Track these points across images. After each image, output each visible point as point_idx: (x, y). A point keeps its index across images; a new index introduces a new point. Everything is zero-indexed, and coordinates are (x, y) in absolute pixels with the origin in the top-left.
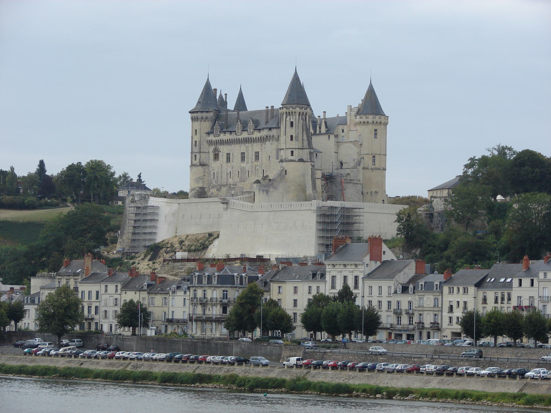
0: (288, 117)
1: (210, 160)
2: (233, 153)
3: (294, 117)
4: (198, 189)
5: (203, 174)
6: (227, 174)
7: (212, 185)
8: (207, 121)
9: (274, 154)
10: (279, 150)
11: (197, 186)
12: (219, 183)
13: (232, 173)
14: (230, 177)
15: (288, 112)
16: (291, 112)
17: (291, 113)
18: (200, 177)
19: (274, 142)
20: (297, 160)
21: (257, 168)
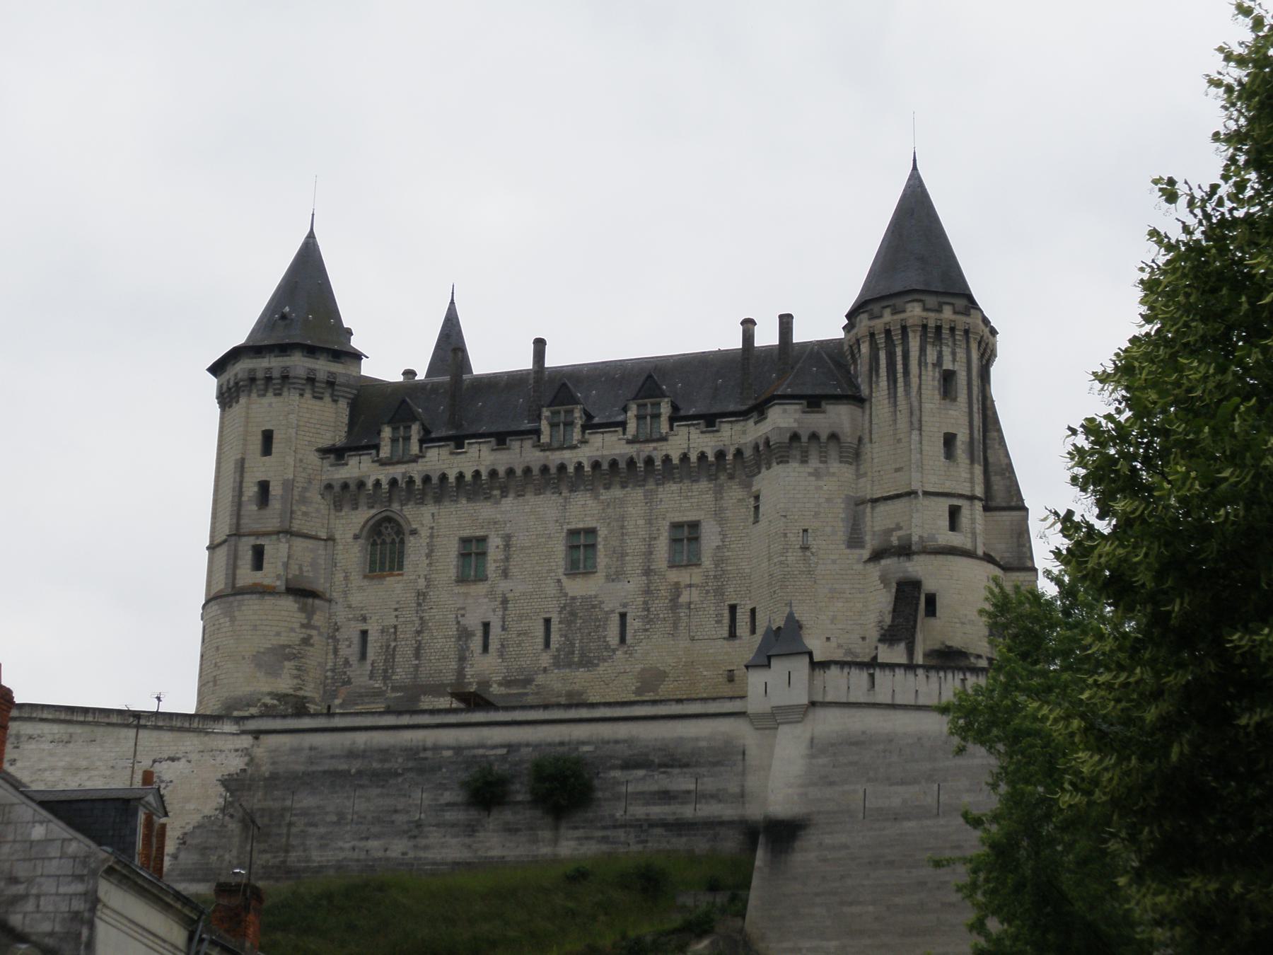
0: (931, 355)
1: (339, 576)
2: (507, 538)
3: (961, 354)
4: (268, 700)
5: (303, 633)
6: (464, 634)
7: (344, 691)
8: (327, 398)
9: (835, 522)
10: (859, 505)
11: (267, 689)
12: (401, 674)
13: (495, 630)
14: (485, 648)
15: (932, 324)
16: (946, 326)
17: (945, 332)
18: (284, 647)
19: (835, 466)
20: (980, 552)
21: (684, 599)
